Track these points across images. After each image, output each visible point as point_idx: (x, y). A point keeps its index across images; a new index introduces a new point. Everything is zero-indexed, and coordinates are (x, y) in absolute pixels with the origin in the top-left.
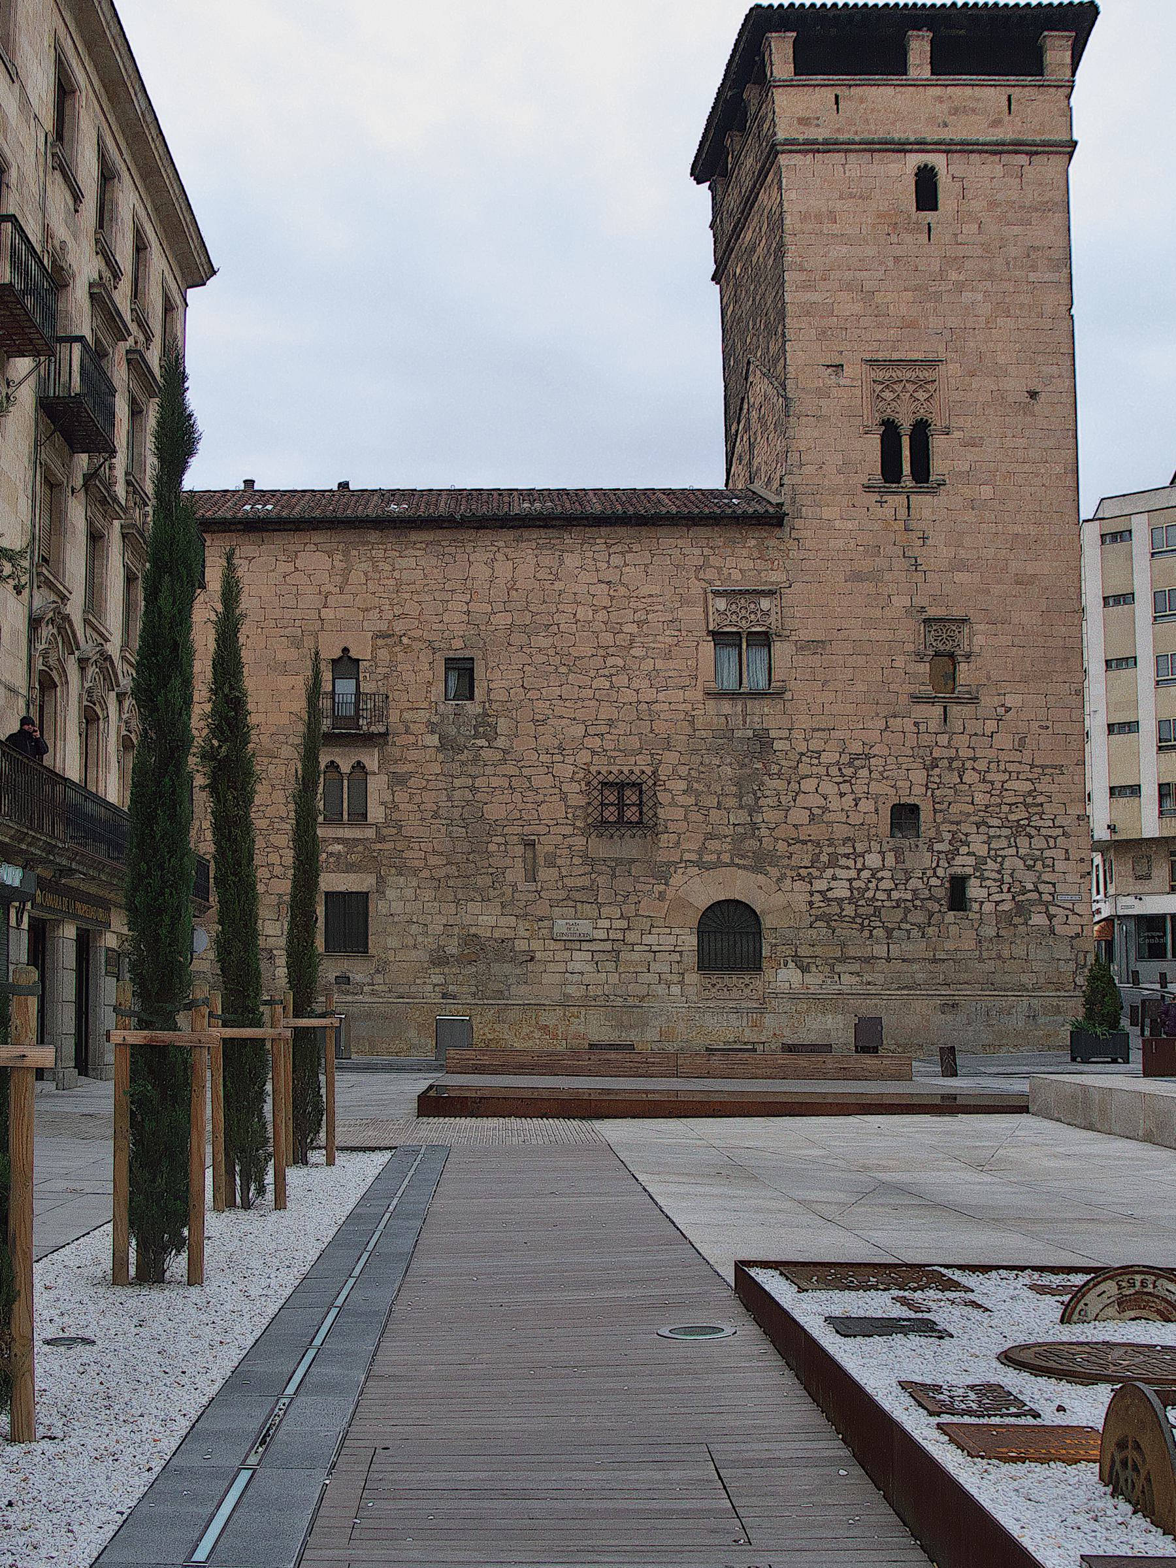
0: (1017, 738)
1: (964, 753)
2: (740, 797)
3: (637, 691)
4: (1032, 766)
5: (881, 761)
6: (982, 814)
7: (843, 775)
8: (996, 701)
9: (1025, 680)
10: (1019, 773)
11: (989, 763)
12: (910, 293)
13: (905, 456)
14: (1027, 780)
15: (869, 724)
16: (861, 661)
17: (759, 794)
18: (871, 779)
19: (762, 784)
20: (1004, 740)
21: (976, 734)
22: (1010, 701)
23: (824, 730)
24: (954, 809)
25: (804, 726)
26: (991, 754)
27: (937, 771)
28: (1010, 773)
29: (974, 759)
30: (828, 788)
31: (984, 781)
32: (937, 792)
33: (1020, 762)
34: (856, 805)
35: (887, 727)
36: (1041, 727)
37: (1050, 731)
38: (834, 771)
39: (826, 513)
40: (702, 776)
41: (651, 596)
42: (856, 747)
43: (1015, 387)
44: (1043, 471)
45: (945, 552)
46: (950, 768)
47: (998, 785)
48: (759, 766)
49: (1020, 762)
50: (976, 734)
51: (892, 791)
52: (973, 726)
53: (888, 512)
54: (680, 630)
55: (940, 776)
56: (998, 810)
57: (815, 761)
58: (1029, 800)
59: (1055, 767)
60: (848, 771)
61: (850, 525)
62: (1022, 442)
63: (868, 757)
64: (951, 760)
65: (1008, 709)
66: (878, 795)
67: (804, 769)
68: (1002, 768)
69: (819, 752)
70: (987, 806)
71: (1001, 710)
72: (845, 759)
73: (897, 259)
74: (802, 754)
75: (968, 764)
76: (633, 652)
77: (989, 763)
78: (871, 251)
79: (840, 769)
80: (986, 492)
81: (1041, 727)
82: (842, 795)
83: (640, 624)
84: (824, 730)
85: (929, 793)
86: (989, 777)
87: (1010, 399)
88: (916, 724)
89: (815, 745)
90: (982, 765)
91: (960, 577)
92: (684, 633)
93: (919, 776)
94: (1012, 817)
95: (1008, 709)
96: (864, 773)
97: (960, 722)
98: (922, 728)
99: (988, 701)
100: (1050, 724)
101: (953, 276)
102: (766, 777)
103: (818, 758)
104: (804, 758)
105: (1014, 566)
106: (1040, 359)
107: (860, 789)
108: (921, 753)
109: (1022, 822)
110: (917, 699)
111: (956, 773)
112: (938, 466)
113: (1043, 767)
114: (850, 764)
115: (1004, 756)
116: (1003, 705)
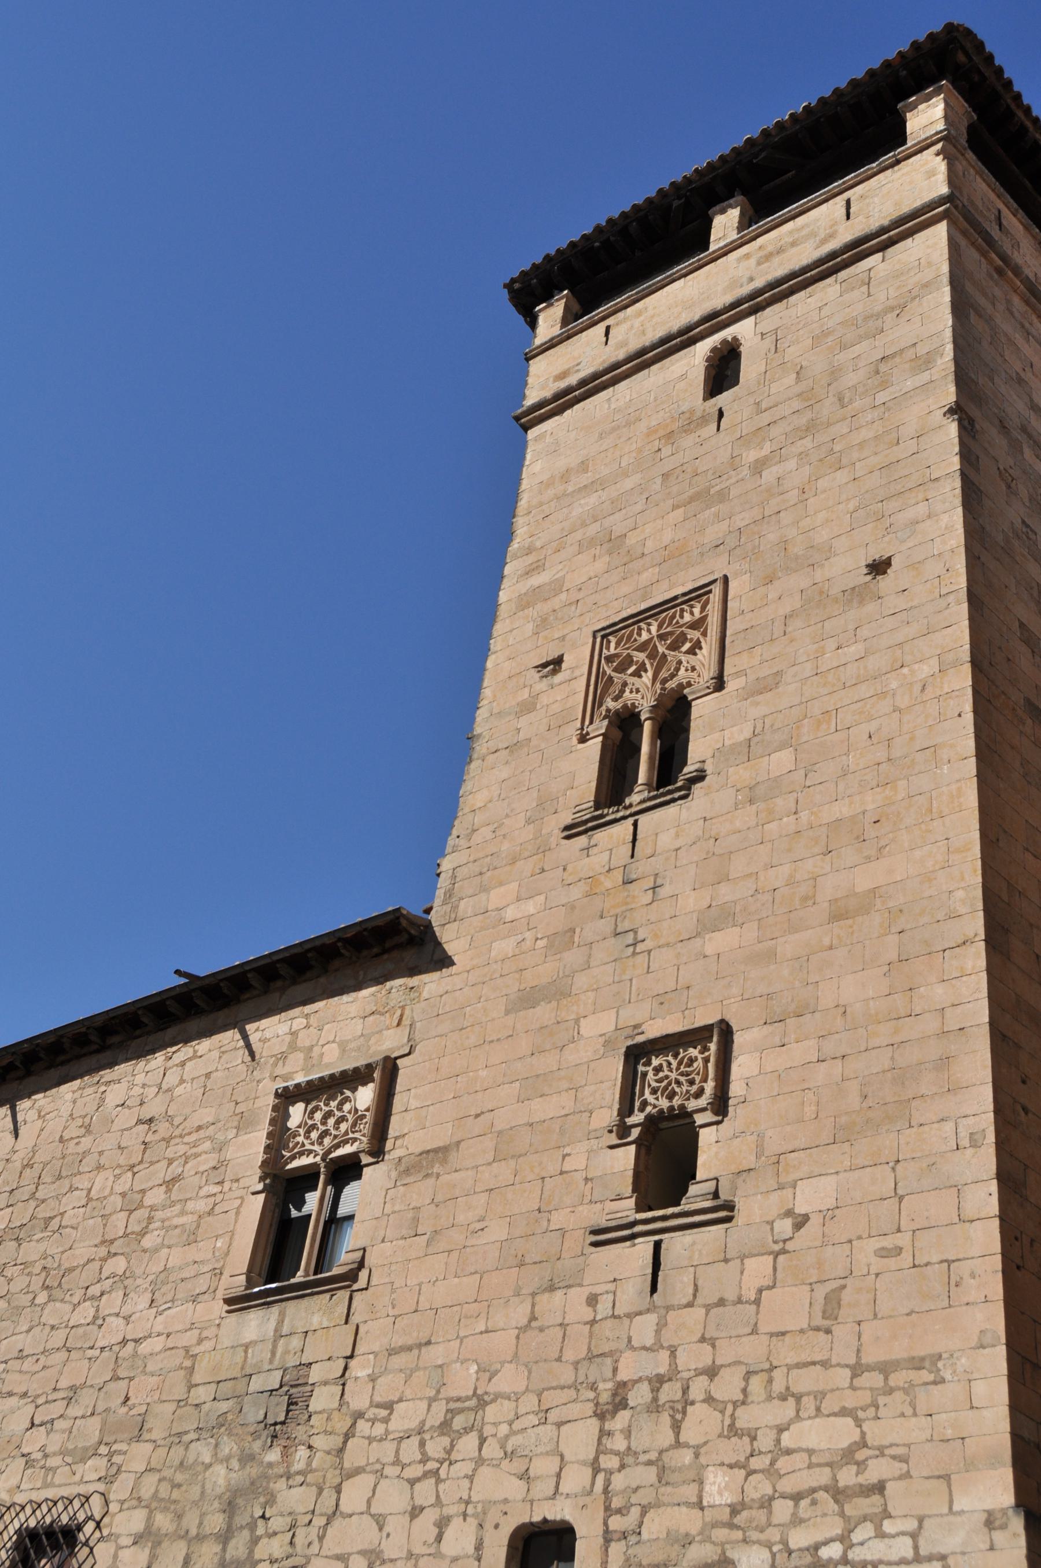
0: (821, 1291)
1: (693, 1357)
2: (225, 1537)
3: (127, 1319)
4: (857, 1370)
5: (508, 1405)
6: (720, 1534)
7: (425, 1459)
8: (775, 1203)
9: (843, 1135)
10: (820, 1396)
11: (748, 1375)
12: (681, 510)
13: (644, 754)
14: (843, 1412)
15: (498, 1319)
16: (504, 1171)
17: (260, 1531)
18: (480, 1461)
19: (271, 1499)
20: (791, 1307)
21: (721, 1302)
22: (809, 1197)
23: (410, 1349)
24: (654, 1526)
25: (376, 1347)
26: (753, 1350)
27: (623, 1417)
28: (798, 1398)
29: (712, 1372)
30: (393, 1498)
31: (733, 1431)
32: (619, 1481)
33: (825, 1364)
34: (439, 1538)
35: (533, 1318)
36: (883, 1253)
37: (906, 1259)
38: (410, 1450)
39: (495, 898)
40: (176, 1494)
41: (199, 1128)
42: (463, 1380)
43: (847, 566)
44: (894, 685)
45: (692, 902)
46: (654, 1407)
47: (766, 1441)
48: (273, 1456)
49: (825, 1364)
50: (721, 1302)
51: (515, 1489)
52: (719, 1281)
53: (598, 860)
54: (221, 1183)
55: (628, 1433)
56: (761, 1516)
57: (379, 1429)
58: (847, 1477)
59: (917, 1364)
60: (436, 1447)
61: (530, 907)
62: (854, 650)
63: (482, 1402)
64: (658, 1382)
65: (801, 1222)
66: (488, 1504)
67: (356, 1453)
68: (778, 1387)
69: (389, 1406)
70: (734, 1510)
71: (785, 1226)
72: (439, 1411)
73: (665, 476)
74: (359, 1415)
75: (698, 1388)
76: (147, 1242)
77: (748, 1375)
78: (628, 483)
79: (422, 1444)
80: (782, 760)
81: (883, 1253)
82: (415, 1512)
83: (170, 1184)
84: (410, 1349)
85: (600, 1478)
86: (745, 1418)
87: (835, 591)
88: (592, 1300)
89: (387, 1387)
90: (728, 1386)
91: (716, 942)
92: (227, 1185)
93: (580, 1439)
94: (799, 1539)
95: (801, 1222)
96: (468, 1444)
97: (687, 1278)
98: (604, 1307)
99: (752, 1208)
100: (903, 1240)
101: (751, 455)
102: (282, 1484)
103: (386, 1420)
104: (361, 1424)
105: (830, 888)
106: (893, 505)
107: (452, 1490)
108: (593, 1374)
109: (825, 1553)
110: (603, 1237)
111: (665, 1419)
112: (699, 749)
113: (885, 1369)
114: (445, 1427)
115: (786, 1353)
116: (789, 1213)
